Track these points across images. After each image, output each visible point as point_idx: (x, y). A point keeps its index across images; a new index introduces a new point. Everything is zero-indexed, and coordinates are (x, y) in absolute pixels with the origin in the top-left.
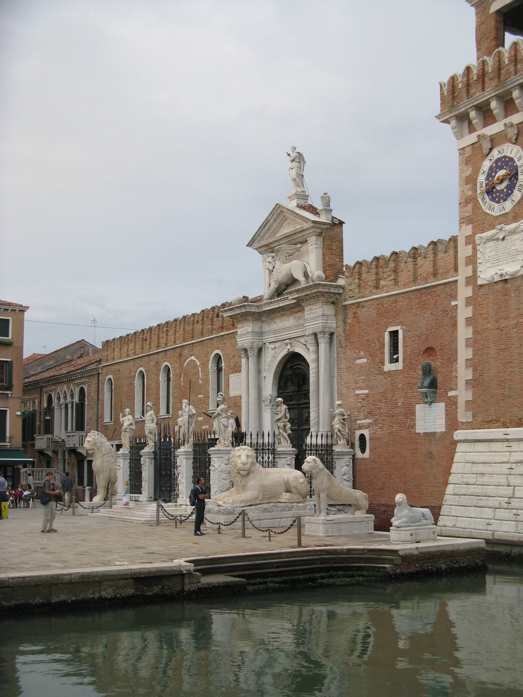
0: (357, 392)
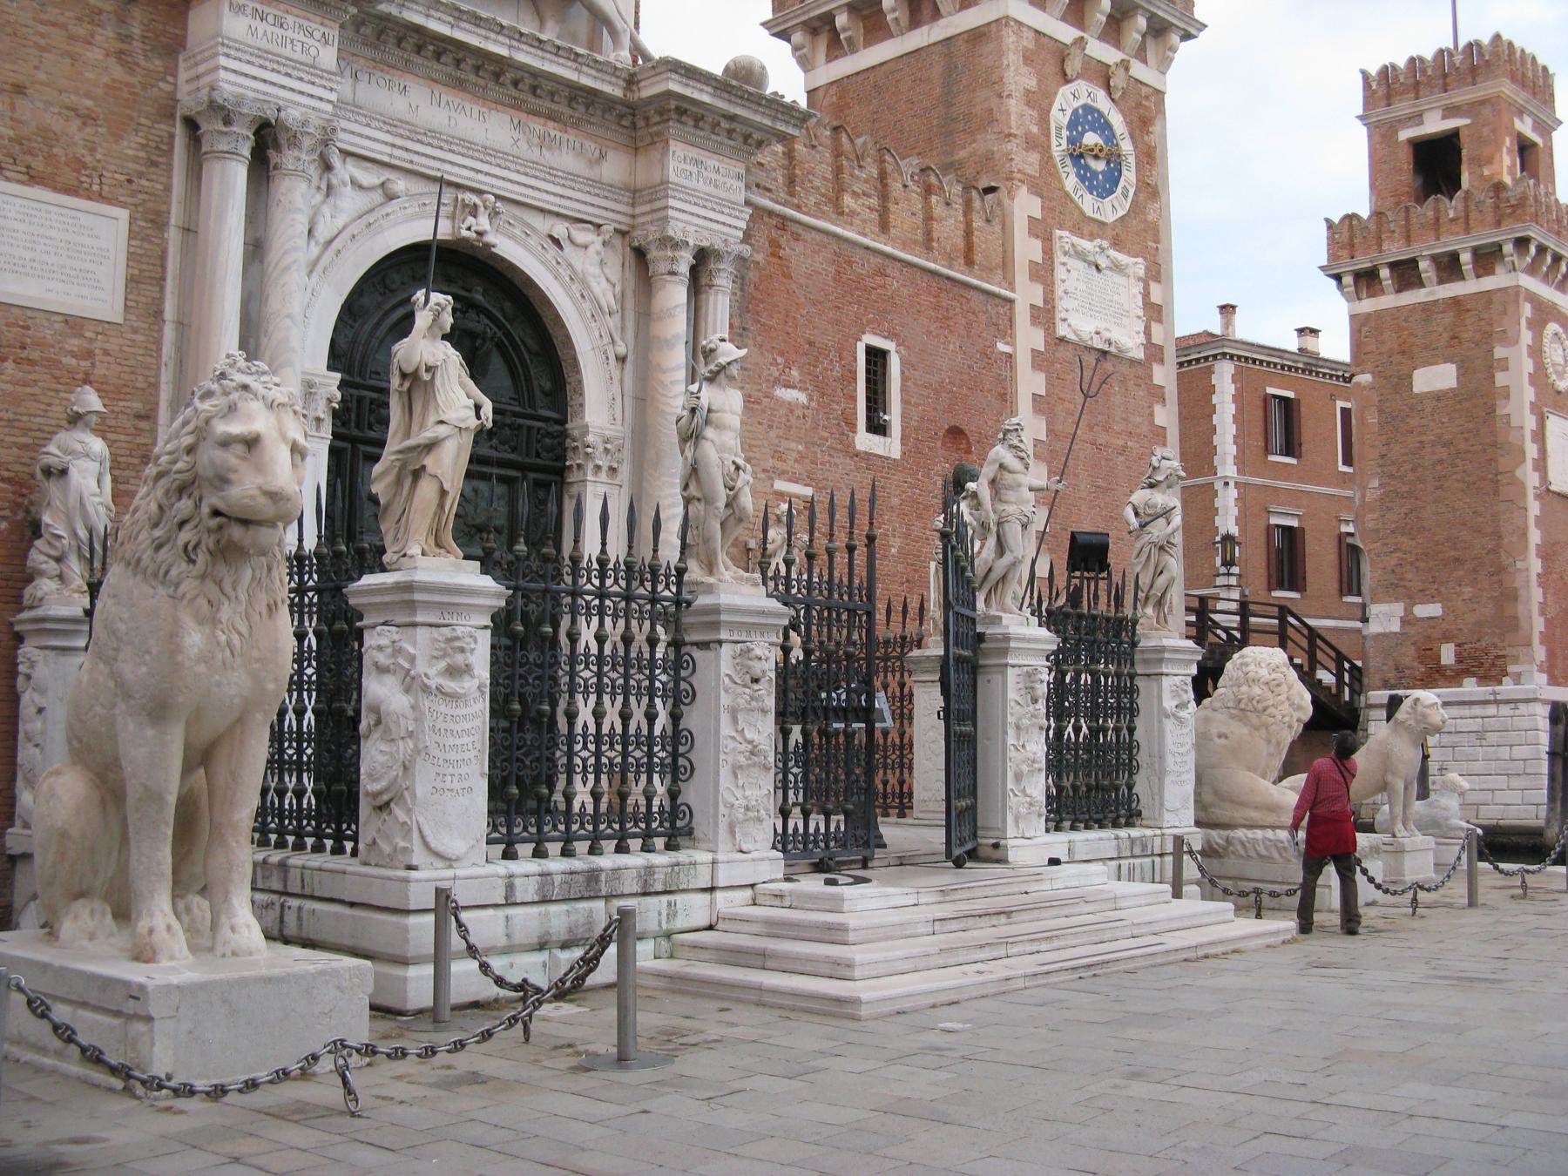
0: (781, 485)
